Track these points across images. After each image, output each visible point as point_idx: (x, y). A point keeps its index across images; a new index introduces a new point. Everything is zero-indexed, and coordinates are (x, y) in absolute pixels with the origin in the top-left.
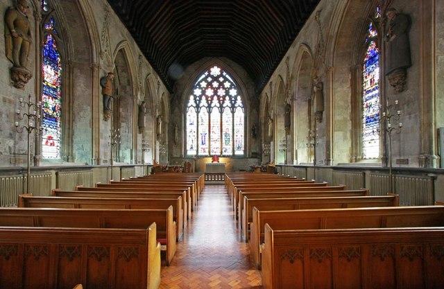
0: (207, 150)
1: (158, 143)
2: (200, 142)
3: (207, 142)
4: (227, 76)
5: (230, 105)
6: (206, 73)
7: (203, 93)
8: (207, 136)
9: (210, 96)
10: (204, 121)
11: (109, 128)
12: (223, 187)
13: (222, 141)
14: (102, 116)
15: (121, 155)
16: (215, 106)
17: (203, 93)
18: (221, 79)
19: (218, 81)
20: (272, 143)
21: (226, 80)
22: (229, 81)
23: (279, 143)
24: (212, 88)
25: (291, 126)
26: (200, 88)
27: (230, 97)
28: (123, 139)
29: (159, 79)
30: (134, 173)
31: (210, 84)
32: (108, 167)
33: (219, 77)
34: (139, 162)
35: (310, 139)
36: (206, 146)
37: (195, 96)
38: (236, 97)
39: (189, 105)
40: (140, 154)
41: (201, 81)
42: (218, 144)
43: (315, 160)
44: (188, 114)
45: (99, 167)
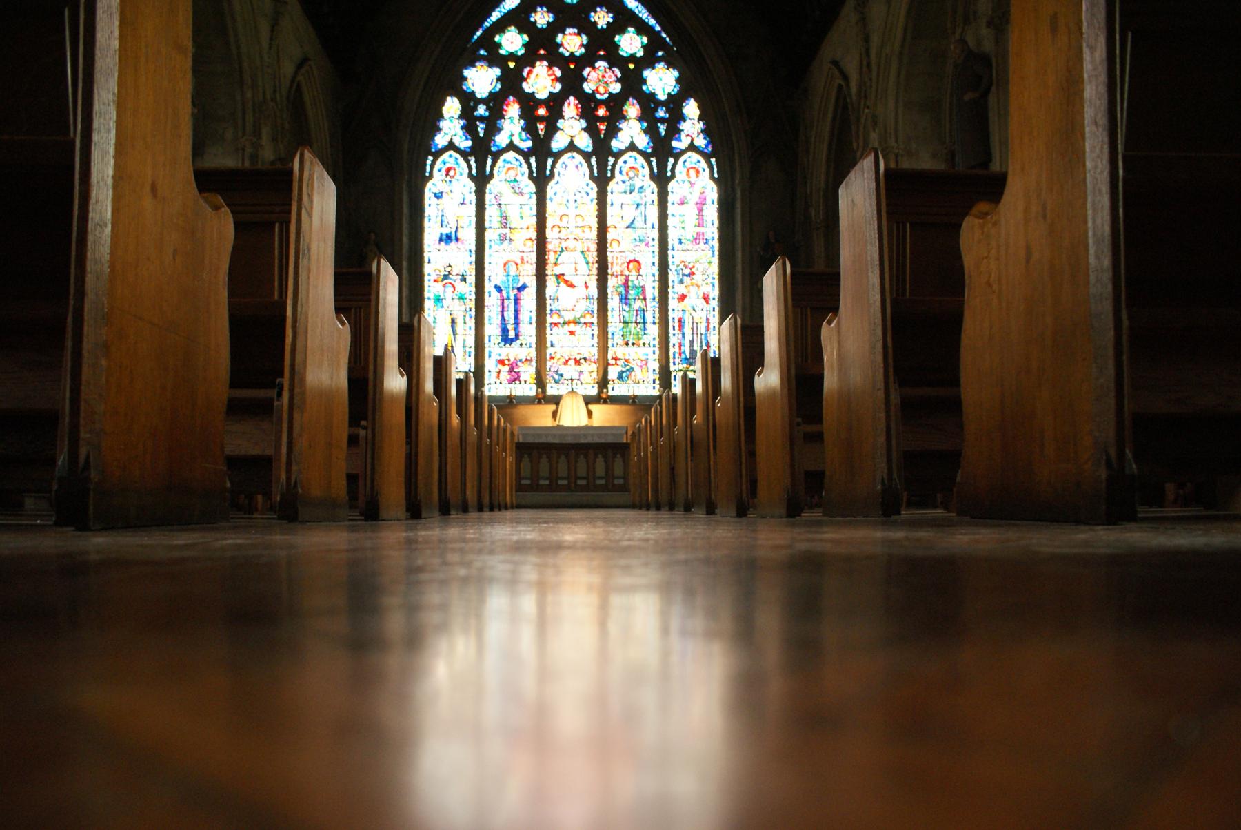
0: (528, 372)
2: (492, 330)
3: (528, 331)
5: (643, 142)
7: (511, 83)
9: (542, 95)
10: (514, 221)
16: (572, 147)
17: (511, 83)
19: (586, 27)
21: (625, 19)
22: (642, 28)
24: (555, 58)
26: (495, 58)
27: (648, 103)
36: (524, 350)
37: (468, 101)
38: (675, 104)
39: (440, 140)
41: (500, 26)
42: (586, 344)
44: (430, 189)
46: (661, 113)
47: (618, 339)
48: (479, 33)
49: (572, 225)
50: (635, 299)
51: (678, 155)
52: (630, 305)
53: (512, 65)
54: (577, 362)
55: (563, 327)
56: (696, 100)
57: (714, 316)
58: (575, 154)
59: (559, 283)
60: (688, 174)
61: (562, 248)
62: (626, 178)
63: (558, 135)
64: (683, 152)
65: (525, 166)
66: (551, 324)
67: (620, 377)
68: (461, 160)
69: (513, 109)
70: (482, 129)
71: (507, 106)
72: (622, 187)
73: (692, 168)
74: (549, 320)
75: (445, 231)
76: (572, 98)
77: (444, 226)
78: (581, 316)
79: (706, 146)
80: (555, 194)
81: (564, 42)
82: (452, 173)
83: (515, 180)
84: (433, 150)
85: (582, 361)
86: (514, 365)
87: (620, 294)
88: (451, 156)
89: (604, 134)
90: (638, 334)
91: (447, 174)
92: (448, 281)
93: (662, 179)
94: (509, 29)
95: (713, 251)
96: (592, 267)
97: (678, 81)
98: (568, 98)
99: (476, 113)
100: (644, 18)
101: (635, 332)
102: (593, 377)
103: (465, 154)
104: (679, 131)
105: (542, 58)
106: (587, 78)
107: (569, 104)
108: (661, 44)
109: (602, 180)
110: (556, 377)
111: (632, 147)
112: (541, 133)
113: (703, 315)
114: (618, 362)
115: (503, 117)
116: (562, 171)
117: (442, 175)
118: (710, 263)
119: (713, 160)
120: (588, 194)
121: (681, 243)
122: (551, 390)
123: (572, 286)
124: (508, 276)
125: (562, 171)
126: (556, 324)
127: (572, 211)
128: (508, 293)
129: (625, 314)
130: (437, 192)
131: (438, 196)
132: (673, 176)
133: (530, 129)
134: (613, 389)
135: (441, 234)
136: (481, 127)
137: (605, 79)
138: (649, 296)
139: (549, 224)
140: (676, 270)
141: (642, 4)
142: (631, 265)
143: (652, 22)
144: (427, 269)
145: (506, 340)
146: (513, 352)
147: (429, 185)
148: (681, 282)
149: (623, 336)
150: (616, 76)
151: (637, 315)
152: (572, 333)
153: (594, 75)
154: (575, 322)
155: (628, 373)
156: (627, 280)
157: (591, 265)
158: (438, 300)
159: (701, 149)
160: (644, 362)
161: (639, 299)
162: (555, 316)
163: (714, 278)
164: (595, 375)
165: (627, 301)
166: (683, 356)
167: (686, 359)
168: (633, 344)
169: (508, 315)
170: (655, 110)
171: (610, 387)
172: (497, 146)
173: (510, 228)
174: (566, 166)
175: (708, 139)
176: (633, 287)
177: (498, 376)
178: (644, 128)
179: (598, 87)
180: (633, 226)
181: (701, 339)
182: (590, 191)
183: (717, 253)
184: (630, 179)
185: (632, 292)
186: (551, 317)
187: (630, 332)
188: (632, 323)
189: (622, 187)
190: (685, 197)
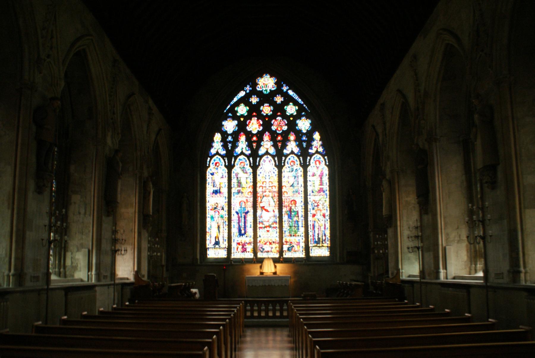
0: (250, 248)
1: (145, 235)
2: (235, 230)
3: (250, 231)
4: (291, 93)
5: (296, 150)
6: (248, 88)
7: (242, 127)
8: (250, 218)
9: (255, 132)
11: (45, 208)
12: (285, 332)
14: (32, 186)
15: (68, 262)
16: (267, 153)
17: (242, 127)
18: (279, 99)
19: (272, 103)
20: (390, 231)
21: (288, 100)
22: (296, 103)
23: (406, 233)
24: (260, 116)
25: (431, 195)
26: (235, 117)
27: (299, 134)
28: (74, 228)
29: (151, 102)
30: (93, 301)
31: (254, 111)
32: (39, 292)
33: (273, 94)
34: (105, 277)
35: (471, 224)
36: (248, 238)
37: (224, 135)
38: (310, 134)
39: (213, 151)
40: (107, 259)
41: (237, 104)
42: (274, 235)
43: (486, 272)
44: (209, 171)
45: (20, 292)
46: (304, 138)
47: (287, 233)
48: (229, 107)
49: (267, 186)
50: (294, 217)
51: (311, 155)
53: (242, 119)
54: (270, 244)
55: (264, 228)
56: (318, 132)
57: (327, 223)
58: (269, 156)
59: (262, 210)
61: (263, 195)
62: (290, 166)
63: (262, 148)
64: (313, 154)
65: (248, 161)
66: (259, 227)
67: (289, 250)
69: (243, 138)
70: (230, 146)
71: (240, 136)
72: (288, 170)
73: (317, 161)
74: (258, 226)
75: (215, 189)
76: (267, 133)
77: (214, 186)
78: (272, 224)
79: (323, 151)
80: (261, 173)
81: (263, 109)
82: (218, 164)
83: (244, 167)
84: (210, 155)
85: (272, 243)
86: (244, 245)
87: (288, 214)
88: (217, 158)
89: (280, 147)
90: (295, 231)
92: (217, 210)
93: (305, 166)
94: (241, 104)
95: (327, 196)
96: (276, 203)
97: (311, 124)
98: (265, 132)
99: (227, 140)
100: (296, 99)
101: (294, 230)
103: (223, 157)
104: (312, 146)
105: (255, 116)
106: (273, 124)
107: (266, 135)
108: (303, 109)
109: (280, 167)
110: (261, 250)
111: (292, 153)
112: (255, 147)
113: (323, 223)
114: (287, 243)
115: (238, 141)
116: (263, 163)
117: (214, 165)
119: (326, 157)
120: (274, 173)
122: (260, 255)
123: (268, 211)
125: (263, 163)
126: (261, 228)
127: (267, 180)
128: (241, 215)
129: (290, 223)
130: (212, 173)
131: (212, 174)
132: (309, 164)
133: (250, 146)
134: (285, 255)
135: (214, 190)
136: (230, 145)
137: (280, 125)
139: (258, 185)
141: (296, 93)
142: (292, 202)
143: (300, 100)
144: (208, 205)
145: (241, 234)
146: (243, 239)
147: (209, 170)
148: (313, 209)
150: (285, 123)
151: (295, 224)
152: (268, 231)
153: (276, 123)
154: (270, 226)
155: (291, 248)
156: (291, 208)
157: (275, 202)
158: (212, 218)
159: (321, 153)
161: (296, 216)
162: (261, 224)
164: (278, 249)
165: (291, 218)
166: (315, 240)
167: (316, 241)
168: (294, 236)
169: (241, 224)
170: (302, 137)
171: (284, 254)
174: (265, 161)
175: (324, 148)
177: (237, 250)
178: (297, 144)
179: (278, 128)
182: (275, 171)
183: (328, 196)
185: (293, 213)
187: (292, 230)
189: (288, 170)
190: (314, 173)
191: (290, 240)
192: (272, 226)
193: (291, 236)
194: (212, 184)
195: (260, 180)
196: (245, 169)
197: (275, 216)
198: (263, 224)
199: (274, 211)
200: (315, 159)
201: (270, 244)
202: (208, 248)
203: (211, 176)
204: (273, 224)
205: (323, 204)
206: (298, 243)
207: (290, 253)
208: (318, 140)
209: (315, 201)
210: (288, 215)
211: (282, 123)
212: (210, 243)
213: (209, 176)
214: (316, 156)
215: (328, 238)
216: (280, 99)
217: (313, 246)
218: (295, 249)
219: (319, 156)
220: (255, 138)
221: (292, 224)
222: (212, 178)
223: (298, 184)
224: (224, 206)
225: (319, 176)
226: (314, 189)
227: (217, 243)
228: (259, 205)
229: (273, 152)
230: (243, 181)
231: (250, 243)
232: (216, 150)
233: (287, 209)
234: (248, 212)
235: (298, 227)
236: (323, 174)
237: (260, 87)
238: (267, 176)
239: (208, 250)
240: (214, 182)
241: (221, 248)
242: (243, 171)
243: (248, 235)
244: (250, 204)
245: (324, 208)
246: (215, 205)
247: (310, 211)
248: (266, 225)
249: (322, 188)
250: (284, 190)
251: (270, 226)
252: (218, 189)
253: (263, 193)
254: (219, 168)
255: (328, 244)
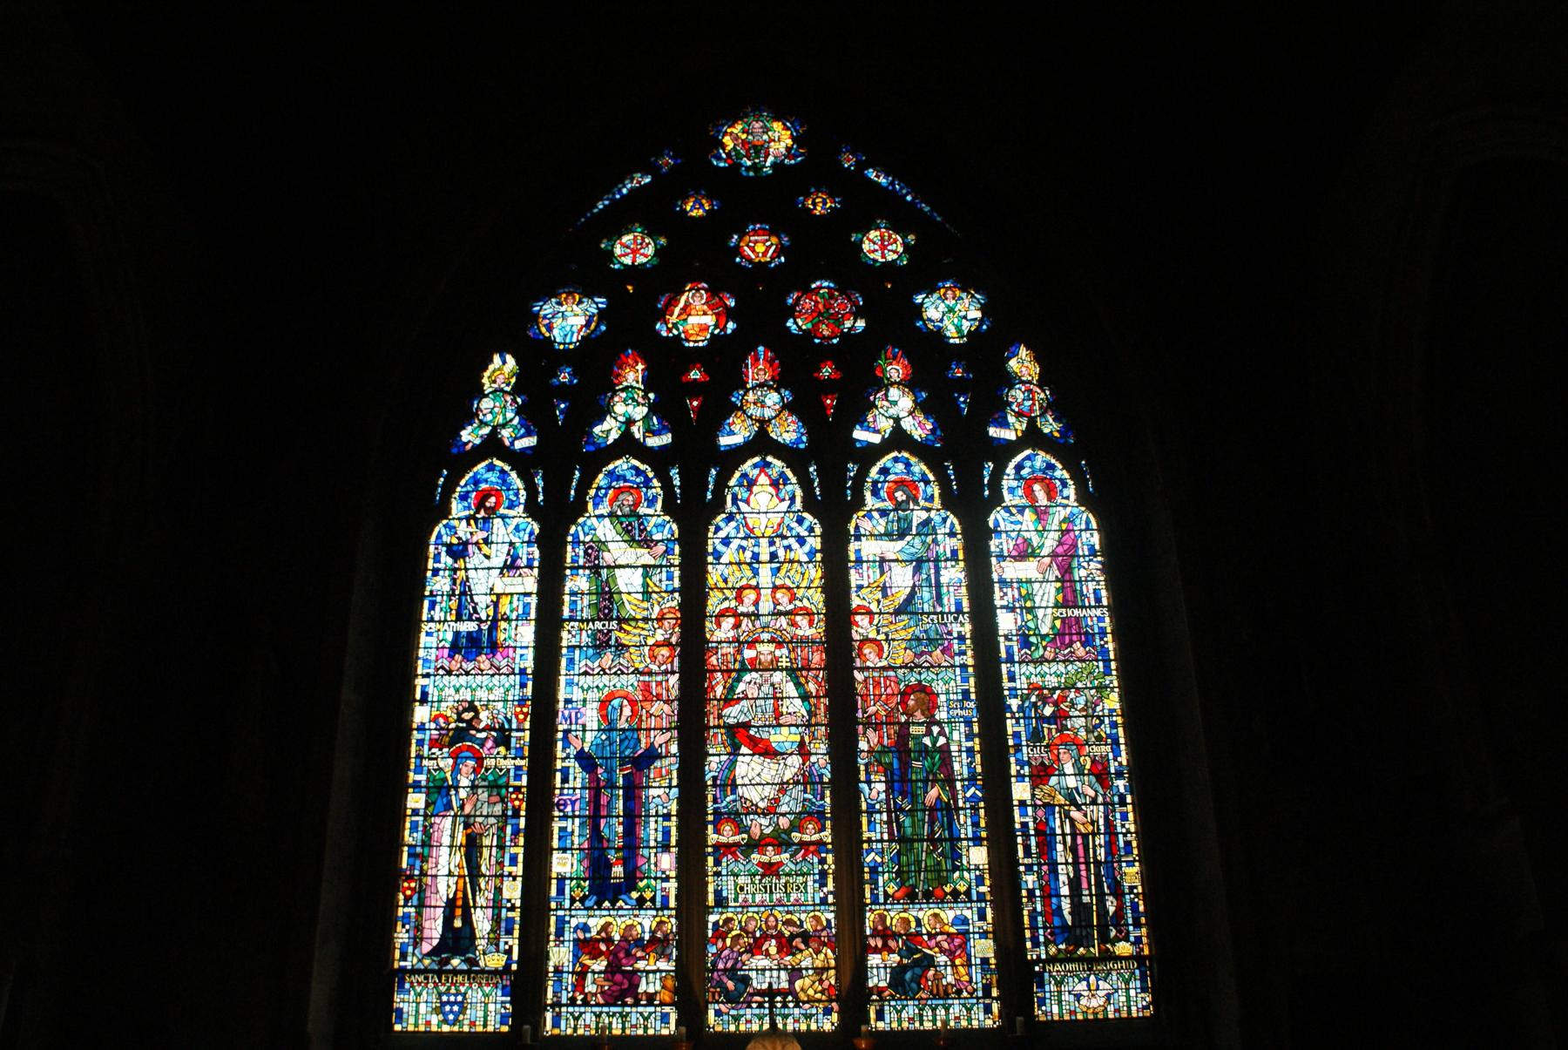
0: (655, 973)
5: (918, 428)
8: (662, 794)
13: (849, 844)
39: (470, 436)
41: (616, 224)
47: (886, 883)
49: (766, 606)
50: (925, 781)
51: (1005, 451)
52: (914, 796)
54: (786, 946)
55: (747, 856)
57: (1124, 817)
60: (1029, 493)
61: (742, 663)
64: (1010, 449)
65: (656, 487)
67: (901, 984)
68: (515, 479)
71: (621, 368)
72: (881, 525)
75: (470, 626)
80: (726, 542)
83: (634, 513)
85: (798, 942)
86: (622, 955)
87: (887, 770)
88: (491, 468)
90: (937, 868)
91: (480, 505)
95: (1107, 662)
102: (826, 984)
107: (756, 359)
111: (898, 439)
113: (1098, 812)
117: (469, 508)
118: (1101, 688)
120: (801, 541)
121: (1025, 642)
124: (610, 730)
127: (765, 577)
132: (997, 499)
133: (665, 409)
134: (880, 1016)
135: (457, 634)
138: (960, 767)
139: (714, 603)
140: (1021, 708)
142: (911, 703)
144: (421, 714)
146: (619, 921)
147: (439, 528)
149: (898, 873)
150: (855, 304)
151: (931, 824)
152: (771, 869)
153: (808, 304)
154: (780, 841)
155: (918, 971)
156: (903, 734)
160: (957, 941)
161: (935, 781)
162: (727, 828)
163: (1114, 725)
165: (908, 787)
166: (1057, 921)
168: (928, 896)
169: (610, 826)
172: (594, 443)
173: (618, 618)
176: (920, 752)
177: (579, 985)
179: (816, 326)
180: (910, 608)
181: (1098, 875)
184: (899, 506)
186: (717, 831)
187: (919, 862)
188: (923, 840)
189: (881, 525)
190: (1027, 542)
191: (906, 922)
192: (796, 836)
193: (911, 897)
194: (454, 604)
195: (725, 581)
196: (642, 523)
197: (807, 779)
198: (740, 828)
199: (803, 751)
200: (1024, 472)
201: (786, 946)
202: (403, 970)
203: (446, 560)
204: (794, 827)
205: (1090, 707)
206: (959, 942)
207: (911, 1010)
208: (1030, 382)
209: (1041, 688)
210: (892, 774)
211: (840, 304)
212: (417, 941)
213: (438, 558)
214: (1028, 458)
215: (1135, 907)
216: (824, 203)
217: (1052, 960)
218: (938, 977)
219: (1041, 458)
220: (695, 375)
221: (913, 825)
222: (455, 570)
223: (939, 598)
224: (510, 722)
225: (1054, 555)
226: (1031, 625)
227: (458, 940)
228: (720, 717)
229: (794, 436)
230: (628, 582)
231: (657, 944)
232: (486, 430)
233: (881, 737)
234: (652, 755)
235: (954, 840)
236: (1075, 546)
237: (724, 156)
238: (765, 557)
239: (401, 986)
240: (463, 593)
241: (483, 971)
242: (627, 530)
243: (648, 895)
244: (663, 711)
245: (1096, 727)
246: (460, 719)
247: (1018, 748)
248: (756, 832)
249: (1078, 619)
250: (862, 627)
251: (780, 841)
252: (485, 627)
253: (740, 651)
254: (497, 522)
255: (1138, 940)
